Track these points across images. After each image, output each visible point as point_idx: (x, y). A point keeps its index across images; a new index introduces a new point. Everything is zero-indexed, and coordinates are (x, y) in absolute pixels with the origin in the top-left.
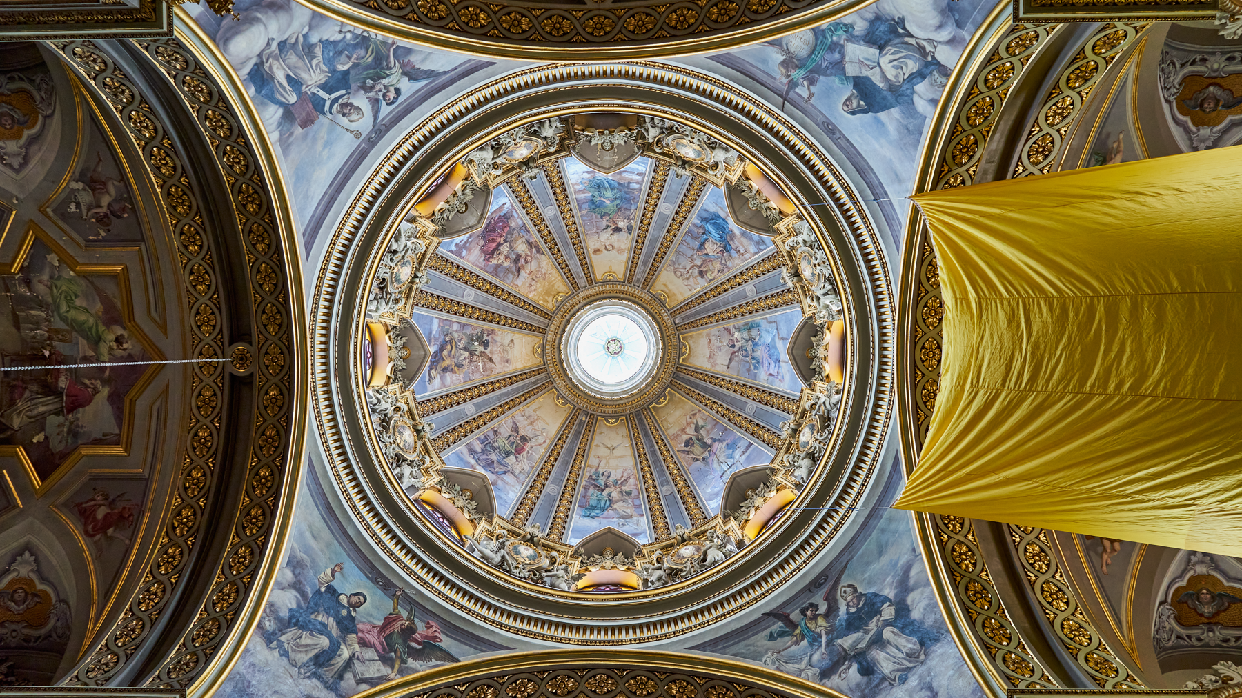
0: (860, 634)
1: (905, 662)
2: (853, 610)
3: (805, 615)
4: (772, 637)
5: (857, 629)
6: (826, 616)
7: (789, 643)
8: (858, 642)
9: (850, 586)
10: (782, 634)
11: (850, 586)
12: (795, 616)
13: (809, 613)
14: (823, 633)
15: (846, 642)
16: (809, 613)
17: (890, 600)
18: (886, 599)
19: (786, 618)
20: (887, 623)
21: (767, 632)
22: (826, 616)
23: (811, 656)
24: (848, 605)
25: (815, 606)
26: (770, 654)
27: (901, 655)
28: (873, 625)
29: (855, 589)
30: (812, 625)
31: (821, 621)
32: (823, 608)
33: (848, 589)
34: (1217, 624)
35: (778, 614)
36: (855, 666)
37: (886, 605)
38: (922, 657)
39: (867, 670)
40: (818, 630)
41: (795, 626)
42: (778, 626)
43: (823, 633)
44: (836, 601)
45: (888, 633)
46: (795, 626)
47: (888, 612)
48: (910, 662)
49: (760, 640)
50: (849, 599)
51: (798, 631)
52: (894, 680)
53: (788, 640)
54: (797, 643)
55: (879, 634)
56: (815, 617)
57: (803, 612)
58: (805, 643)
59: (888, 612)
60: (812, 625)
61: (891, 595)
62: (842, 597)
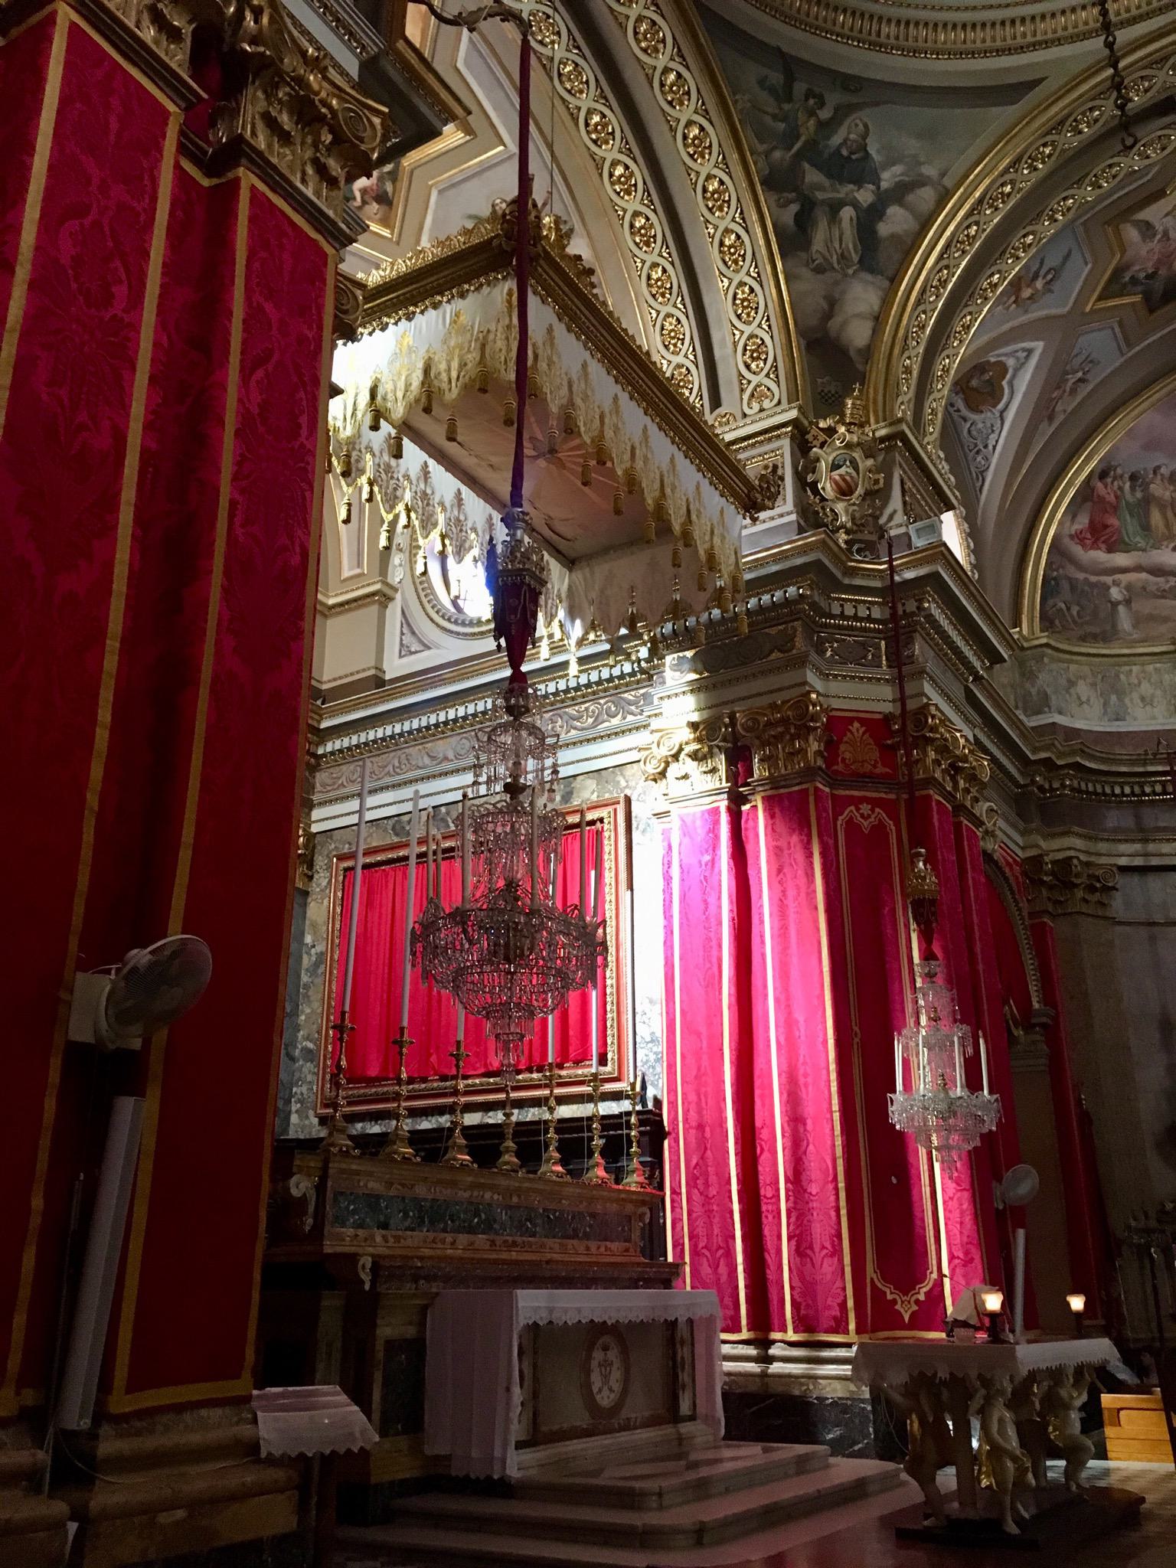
0: (826, 182)
1: (835, 257)
2: (845, 152)
3: (807, 99)
4: (762, 82)
5: (829, 175)
6: (822, 125)
7: (770, 110)
8: (821, 188)
9: (866, 126)
10: (772, 91)
11: (866, 126)
12: (800, 88)
13: (811, 102)
14: (803, 138)
15: (812, 176)
16: (811, 102)
17: (879, 188)
18: (876, 181)
19: (790, 79)
20: (855, 204)
21: (765, 71)
22: (822, 125)
23: (774, 148)
24: (845, 140)
25: (822, 104)
26: (746, 97)
27: (837, 246)
28: (845, 190)
29: (865, 135)
30: (801, 116)
31: (812, 122)
32: (825, 114)
33: (861, 126)
34: (964, 393)
35: (790, 65)
36: (794, 208)
37: (871, 187)
38: (850, 271)
39: (804, 221)
40: (802, 130)
41: (789, 98)
42: (776, 78)
43: (803, 138)
44: (840, 124)
45: (847, 213)
46: (789, 98)
47: (865, 196)
48: (839, 263)
49: (752, 72)
50: (852, 136)
51: (786, 107)
52: (813, 261)
53: (770, 105)
54: (775, 117)
55: (840, 204)
56: (812, 113)
57: (809, 94)
58: (782, 126)
59: (865, 196)
60: (801, 116)
61: (884, 185)
62: (849, 127)
